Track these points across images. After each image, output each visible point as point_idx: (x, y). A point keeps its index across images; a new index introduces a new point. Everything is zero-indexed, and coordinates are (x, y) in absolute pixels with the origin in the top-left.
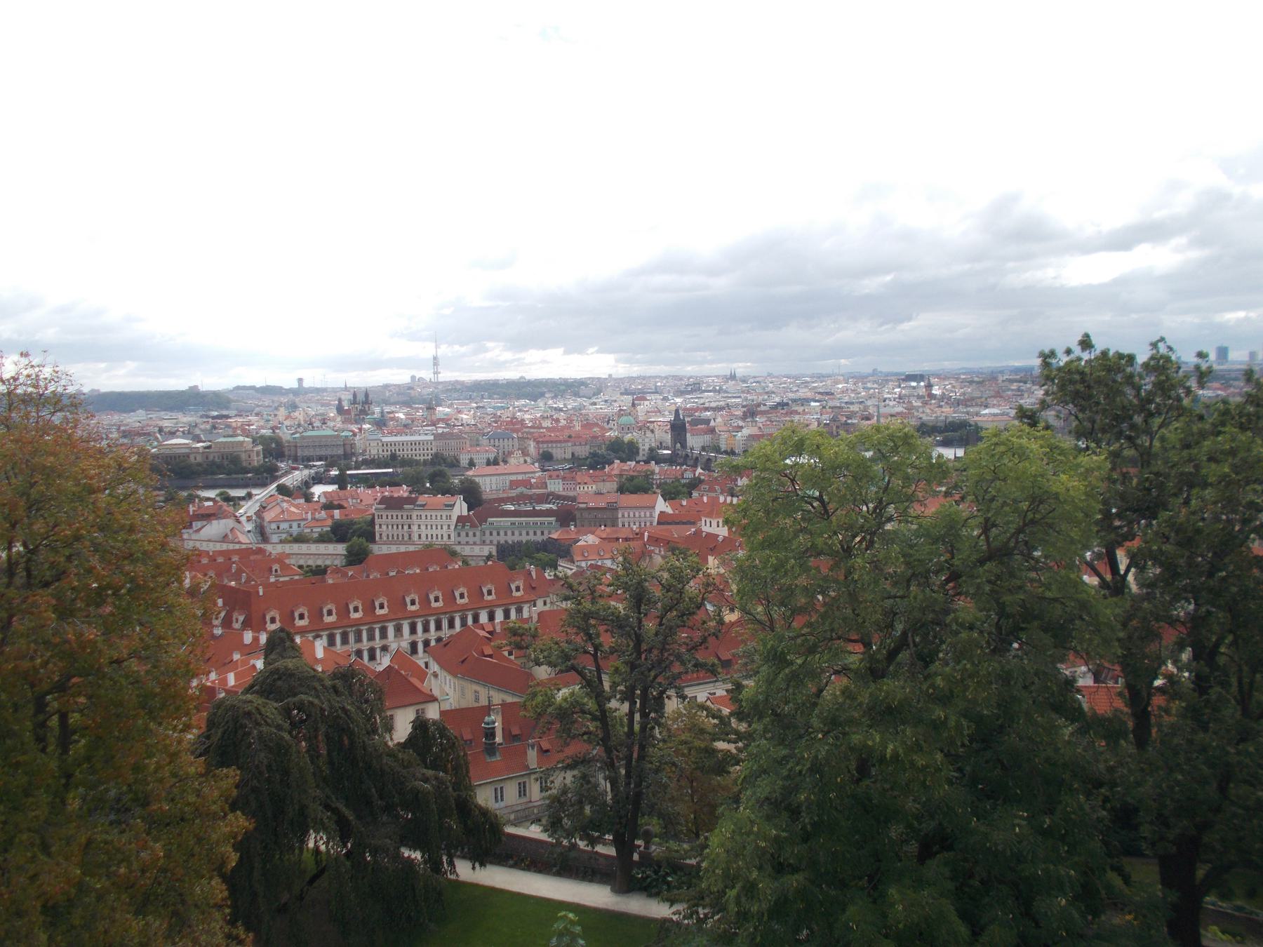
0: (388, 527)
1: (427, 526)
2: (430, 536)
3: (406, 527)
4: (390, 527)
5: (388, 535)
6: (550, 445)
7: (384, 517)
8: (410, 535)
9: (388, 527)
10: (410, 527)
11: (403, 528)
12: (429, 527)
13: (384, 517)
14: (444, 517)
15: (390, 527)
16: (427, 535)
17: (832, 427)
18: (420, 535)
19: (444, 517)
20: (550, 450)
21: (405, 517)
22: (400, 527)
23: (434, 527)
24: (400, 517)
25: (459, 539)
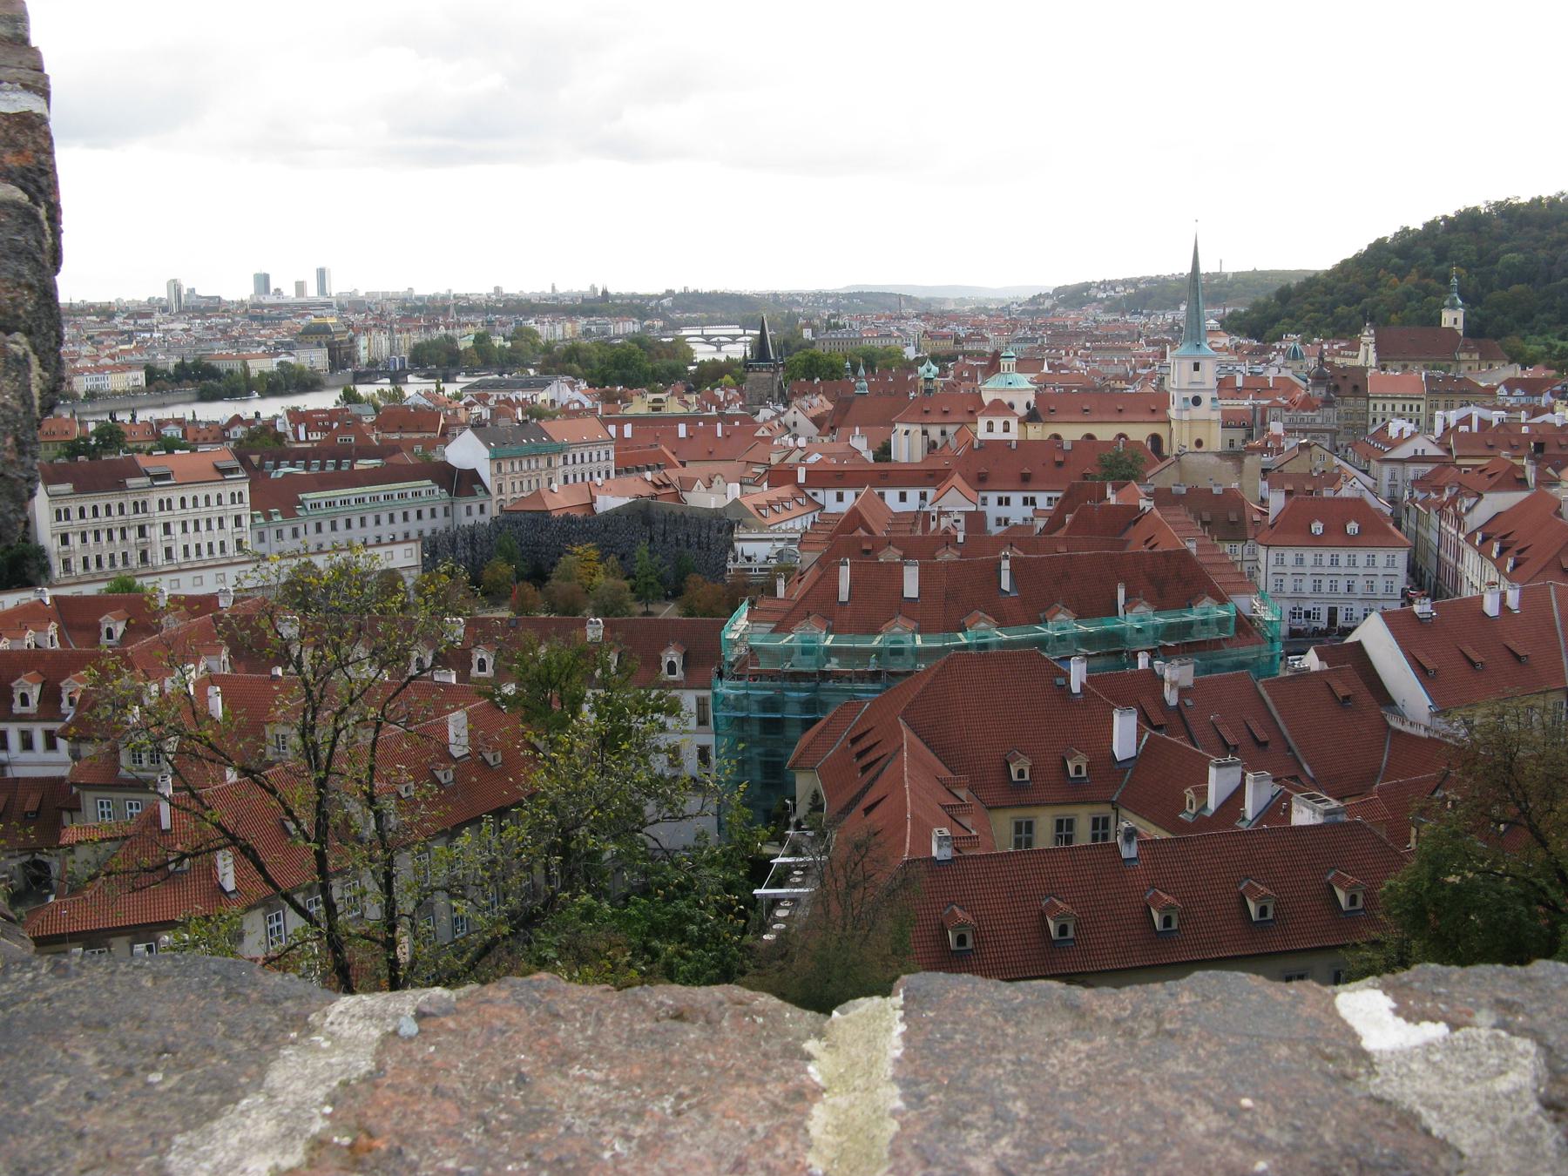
0: (84, 540)
1: (184, 524)
2: (192, 550)
3: (132, 534)
4: (91, 538)
7: (75, 514)
9: (84, 540)
10: (142, 531)
11: (124, 537)
12: (191, 527)
13: (75, 514)
14: (226, 499)
15: (91, 538)
16: (186, 548)
18: (168, 551)
19: (226, 499)
21: (129, 509)
22: (117, 535)
23: (203, 526)
24: (115, 511)
25: (262, 548)
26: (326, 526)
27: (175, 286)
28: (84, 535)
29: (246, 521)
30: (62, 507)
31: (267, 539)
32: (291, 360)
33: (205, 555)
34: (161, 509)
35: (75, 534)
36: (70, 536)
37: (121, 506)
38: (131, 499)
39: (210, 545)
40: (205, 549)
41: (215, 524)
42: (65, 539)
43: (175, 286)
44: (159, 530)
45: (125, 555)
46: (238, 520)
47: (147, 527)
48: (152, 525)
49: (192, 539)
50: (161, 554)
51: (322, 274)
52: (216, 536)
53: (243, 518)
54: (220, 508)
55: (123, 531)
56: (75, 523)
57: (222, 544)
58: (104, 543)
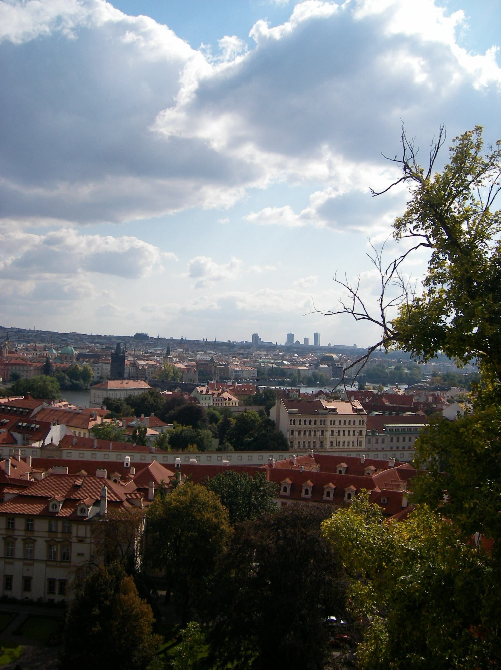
0: (299, 434)
3: (319, 434)
4: (302, 433)
5: (299, 442)
6: (18, 368)
7: (297, 423)
8: (322, 442)
9: (299, 434)
10: (322, 432)
11: (315, 435)
12: (342, 433)
13: (297, 423)
15: (302, 433)
16: (339, 442)
17: (212, 367)
20: (18, 372)
21: (318, 423)
22: (312, 433)
23: (347, 433)
26: (395, 439)
27: (255, 337)
28: (300, 431)
29: (364, 433)
30: (293, 419)
31: (371, 441)
32: (316, 371)
33: (346, 446)
34: (331, 424)
35: (296, 431)
36: (295, 432)
37: (315, 421)
38: (320, 419)
39: (349, 442)
40: (346, 444)
41: (351, 433)
42: (292, 433)
43: (255, 337)
44: (329, 433)
45: (315, 442)
46: (361, 431)
47: (325, 431)
48: (327, 431)
49: (341, 438)
50: (329, 444)
51: (316, 336)
52: (351, 438)
53: (363, 431)
54: (354, 426)
55: (315, 432)
56: (297, 426)
57: (353, 442)
58: (307, 436)
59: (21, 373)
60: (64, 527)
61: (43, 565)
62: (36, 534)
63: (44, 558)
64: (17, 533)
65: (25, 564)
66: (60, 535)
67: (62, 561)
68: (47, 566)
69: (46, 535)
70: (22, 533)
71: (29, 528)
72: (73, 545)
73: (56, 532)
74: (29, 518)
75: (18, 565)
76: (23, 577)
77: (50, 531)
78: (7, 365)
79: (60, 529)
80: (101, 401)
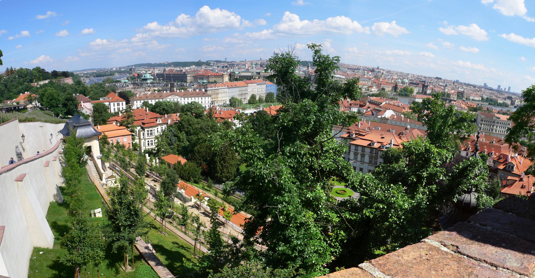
59: (385, 88)
60: (376, 151)
61: (367, 165)
62: (365, 153)
63: (368, 162)
64: (359, 151)
65: (361, 163)
66: (374, 154)
67: (374, 164)
68: (369, 165)
69: (369, 154)
70: (361, 152)
71: (363, 151)
72: (378, 159)
73: (373, 153)
74: (363, 147)
75: (358, 163)
76: (360, 168)
77: (371, 152)
78: (381, 84)
79: (374, 152)
80: (412, 102)
